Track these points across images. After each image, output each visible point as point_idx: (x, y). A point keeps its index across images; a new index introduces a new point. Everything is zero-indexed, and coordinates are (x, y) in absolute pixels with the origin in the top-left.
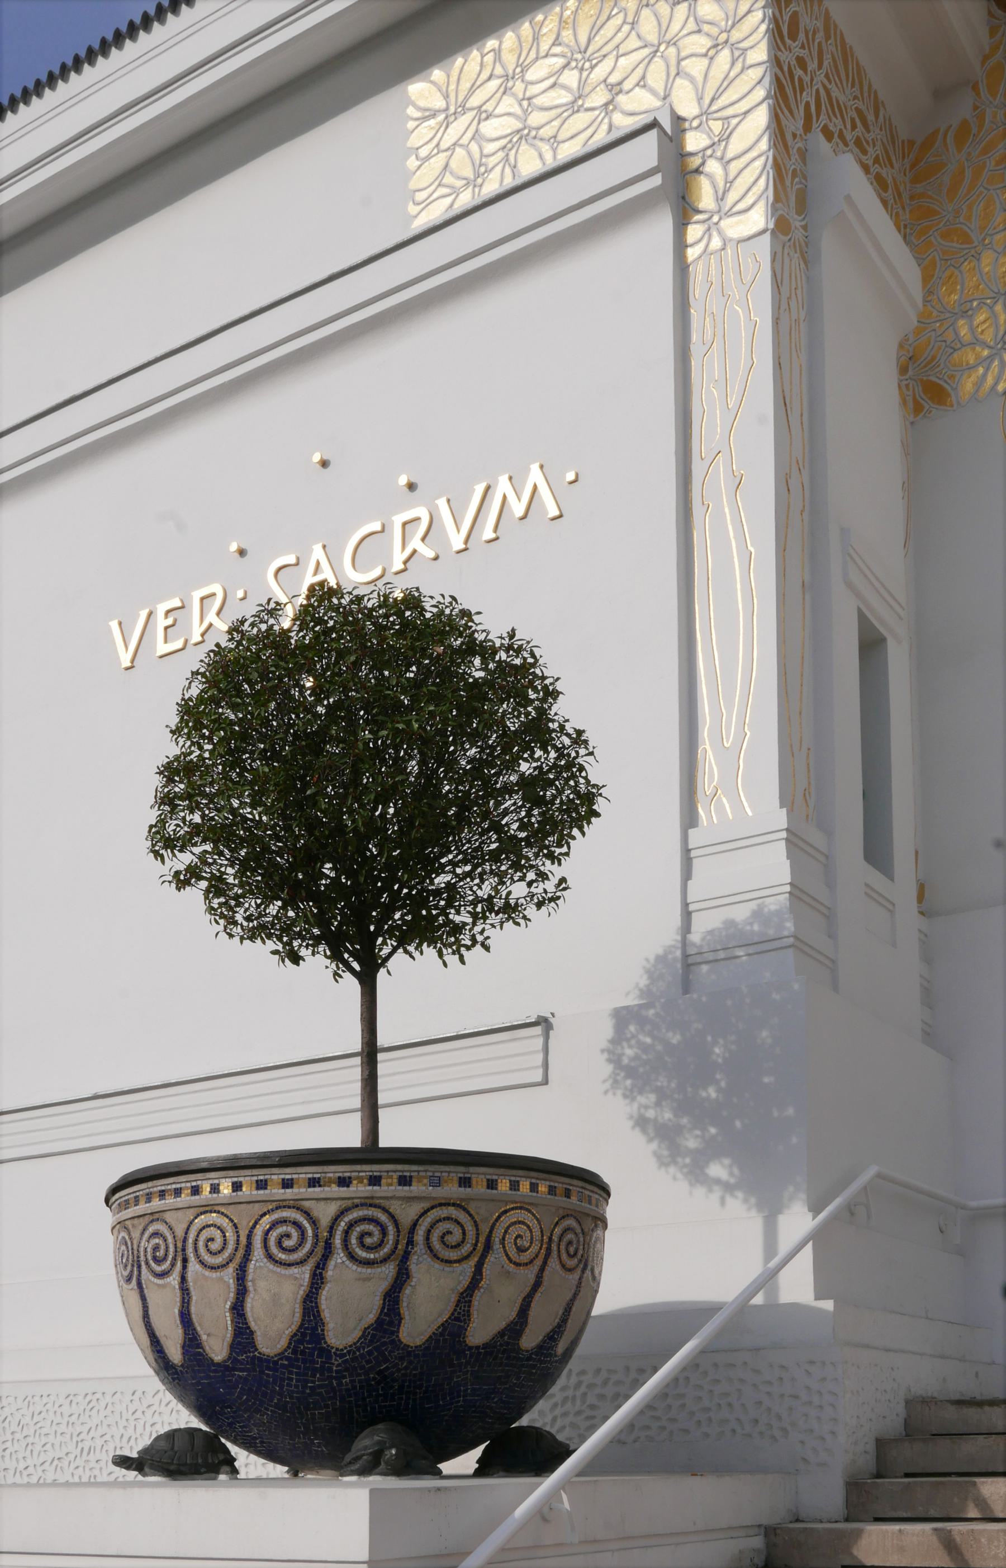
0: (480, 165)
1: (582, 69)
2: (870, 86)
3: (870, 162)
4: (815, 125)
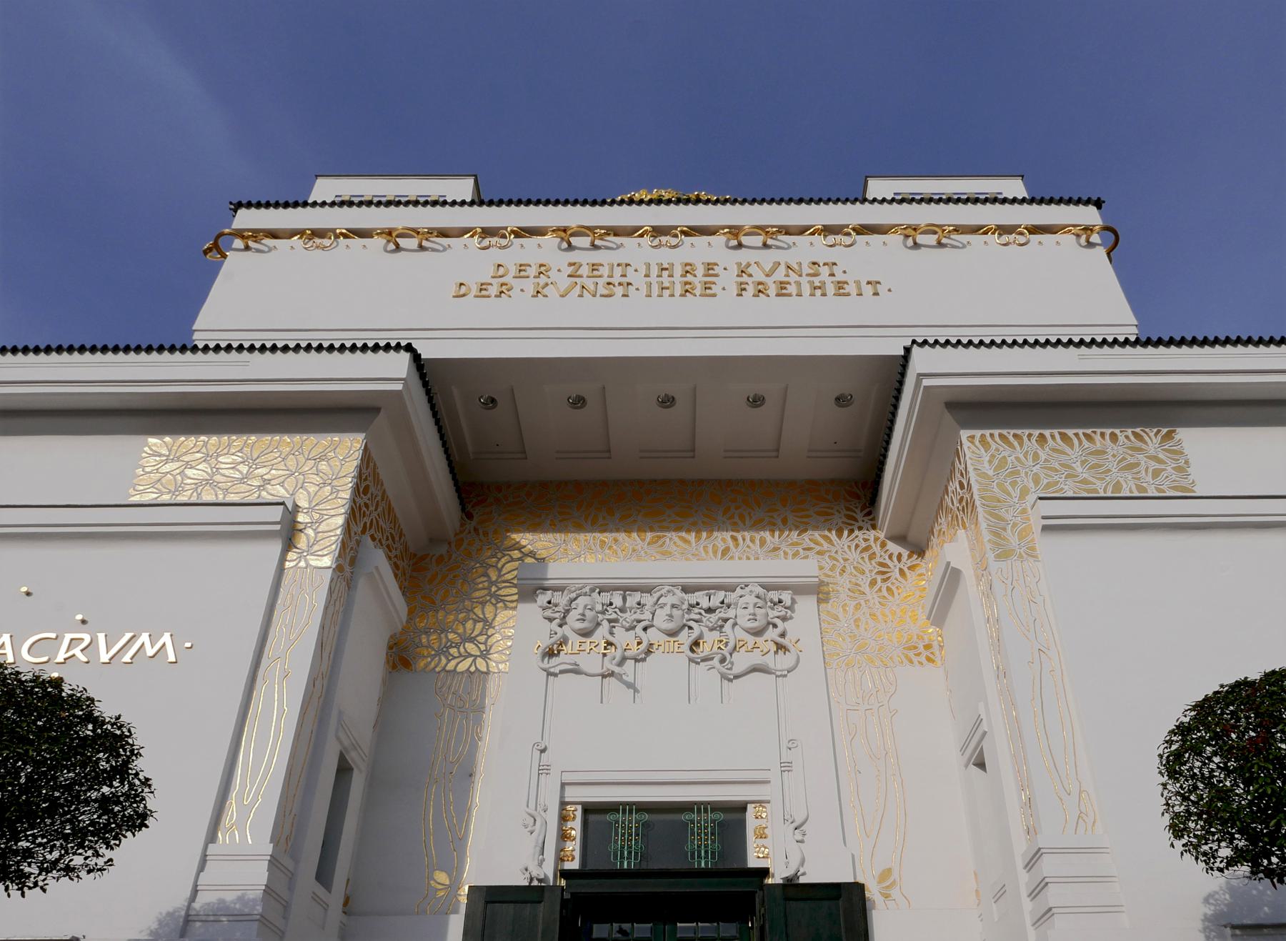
0: (180, 487)
1: (251, 467)
2: (399, 526)
3: (392, 556)
4: (367, 532)
